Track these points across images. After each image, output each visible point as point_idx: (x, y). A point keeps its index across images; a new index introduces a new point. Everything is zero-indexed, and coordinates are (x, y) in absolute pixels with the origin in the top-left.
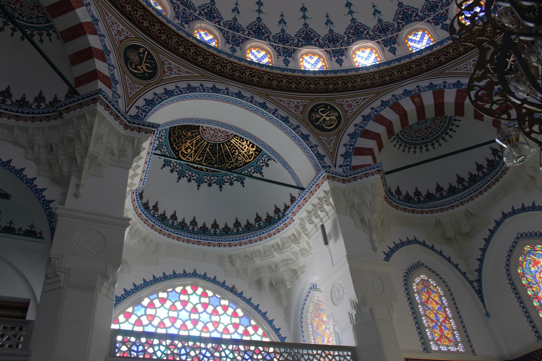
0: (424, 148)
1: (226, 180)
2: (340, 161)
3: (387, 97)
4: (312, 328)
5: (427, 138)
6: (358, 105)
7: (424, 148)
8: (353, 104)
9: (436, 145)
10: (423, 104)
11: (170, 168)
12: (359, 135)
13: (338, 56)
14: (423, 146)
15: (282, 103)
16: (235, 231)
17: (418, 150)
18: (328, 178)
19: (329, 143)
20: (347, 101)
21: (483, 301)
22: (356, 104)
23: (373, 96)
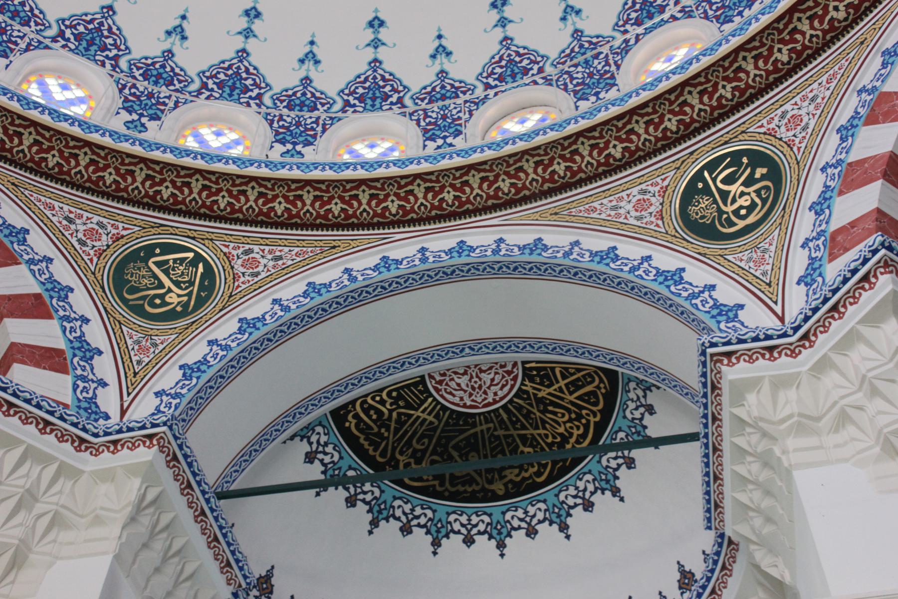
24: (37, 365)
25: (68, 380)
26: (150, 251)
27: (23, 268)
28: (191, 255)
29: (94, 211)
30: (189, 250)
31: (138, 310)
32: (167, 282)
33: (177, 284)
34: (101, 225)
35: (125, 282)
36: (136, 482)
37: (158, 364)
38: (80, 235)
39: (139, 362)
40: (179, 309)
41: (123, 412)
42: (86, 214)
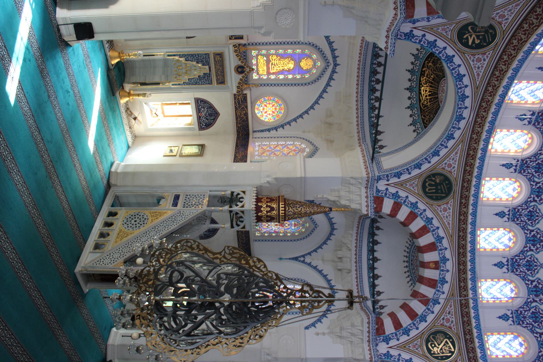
0: (406, 259)
1: (412, 94)
2: (392, 190)
3: (445, 243)
4: (291, 145)
5: (412, 264)
6: (444, 217)
7: (406, 259)
8: (446, 213)
9: (406, 269)
10: (427, 268)
11: (420, 48)
12: (413, 210)
13: (509, 215)
14: (408, 259)
15: (454, 153)
16: (372, 97)
17: (406, 254)
18: (368, 177)
19: (411, 185)
20: (449, 209)
21: (290, 259)
22: (445, 215)
23: (451, 232)
24: (393, 323)
25: (394, 331)
26: (450, 338)
27: (425, 308)
28: (453, 350)
29: (456, 318)
30: (455, 349)
31: (427, 341)
32: (440, 347)
33: (441, 349)
34: (452, 322)
35: (434, 335)
36: (362, 357)
37: (410, 351)
38: (446, 318)
39: (409, 347)
40: (432, 352)
41: (390, 347)
42: (454, 316)
